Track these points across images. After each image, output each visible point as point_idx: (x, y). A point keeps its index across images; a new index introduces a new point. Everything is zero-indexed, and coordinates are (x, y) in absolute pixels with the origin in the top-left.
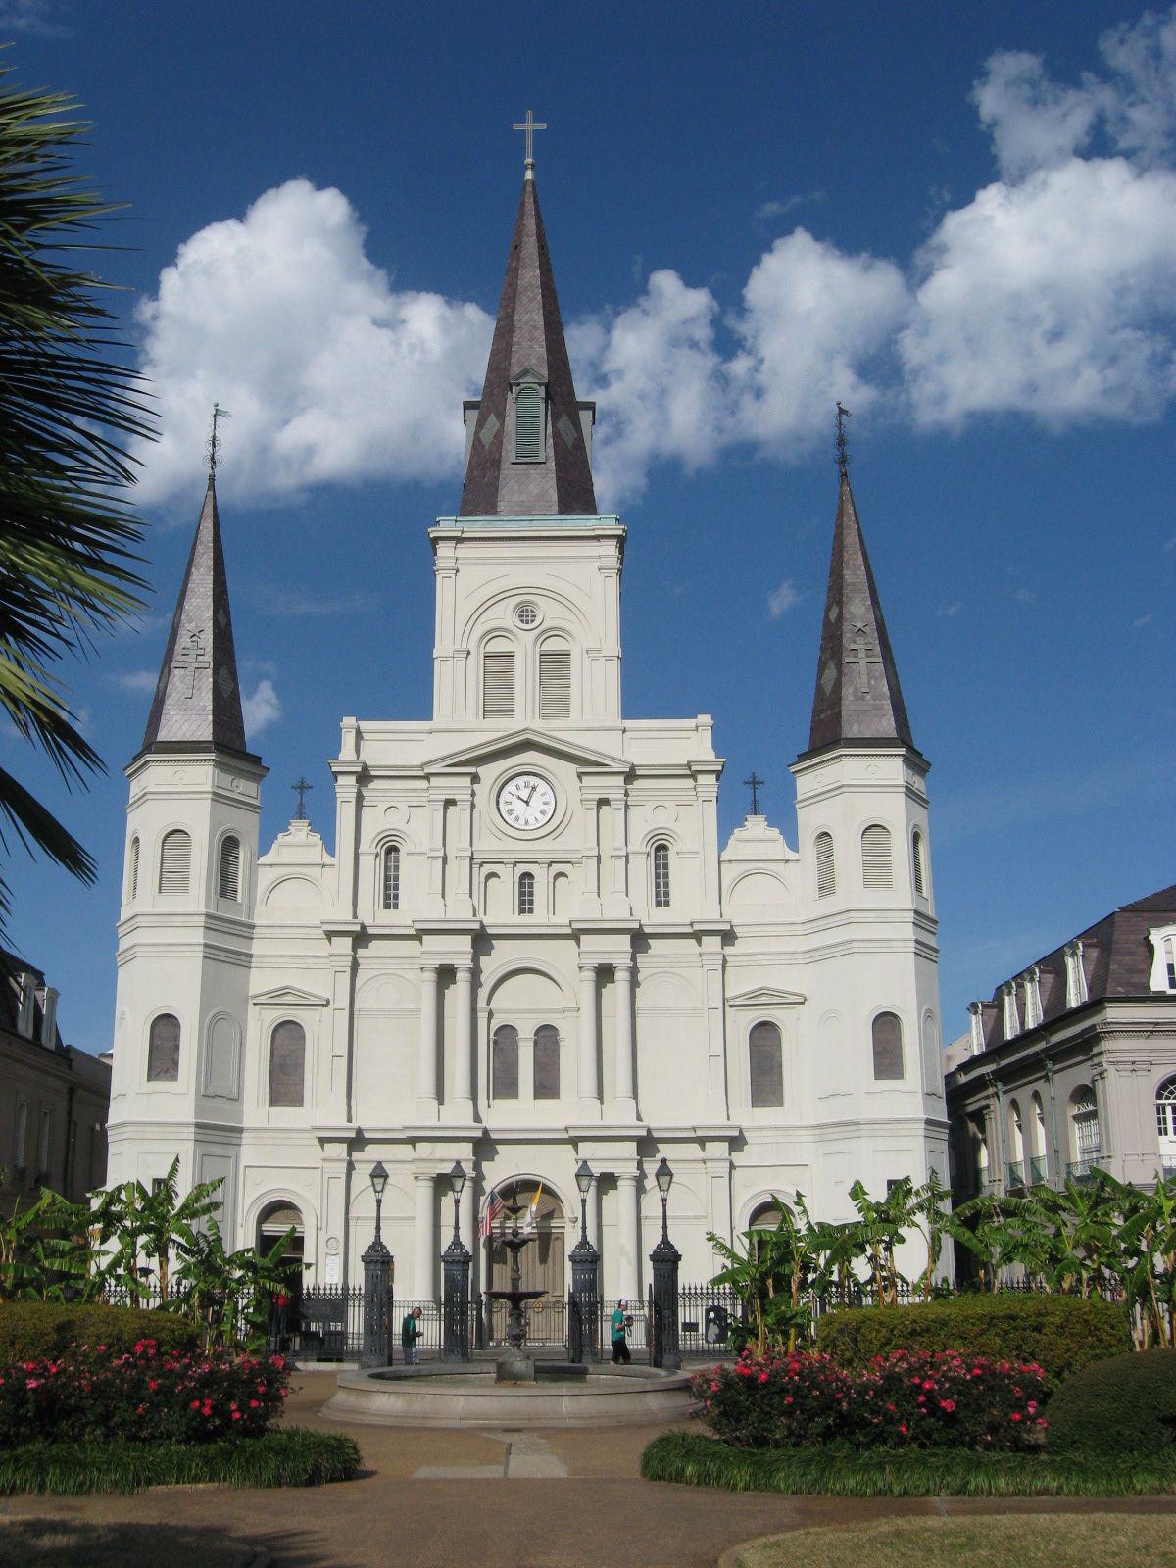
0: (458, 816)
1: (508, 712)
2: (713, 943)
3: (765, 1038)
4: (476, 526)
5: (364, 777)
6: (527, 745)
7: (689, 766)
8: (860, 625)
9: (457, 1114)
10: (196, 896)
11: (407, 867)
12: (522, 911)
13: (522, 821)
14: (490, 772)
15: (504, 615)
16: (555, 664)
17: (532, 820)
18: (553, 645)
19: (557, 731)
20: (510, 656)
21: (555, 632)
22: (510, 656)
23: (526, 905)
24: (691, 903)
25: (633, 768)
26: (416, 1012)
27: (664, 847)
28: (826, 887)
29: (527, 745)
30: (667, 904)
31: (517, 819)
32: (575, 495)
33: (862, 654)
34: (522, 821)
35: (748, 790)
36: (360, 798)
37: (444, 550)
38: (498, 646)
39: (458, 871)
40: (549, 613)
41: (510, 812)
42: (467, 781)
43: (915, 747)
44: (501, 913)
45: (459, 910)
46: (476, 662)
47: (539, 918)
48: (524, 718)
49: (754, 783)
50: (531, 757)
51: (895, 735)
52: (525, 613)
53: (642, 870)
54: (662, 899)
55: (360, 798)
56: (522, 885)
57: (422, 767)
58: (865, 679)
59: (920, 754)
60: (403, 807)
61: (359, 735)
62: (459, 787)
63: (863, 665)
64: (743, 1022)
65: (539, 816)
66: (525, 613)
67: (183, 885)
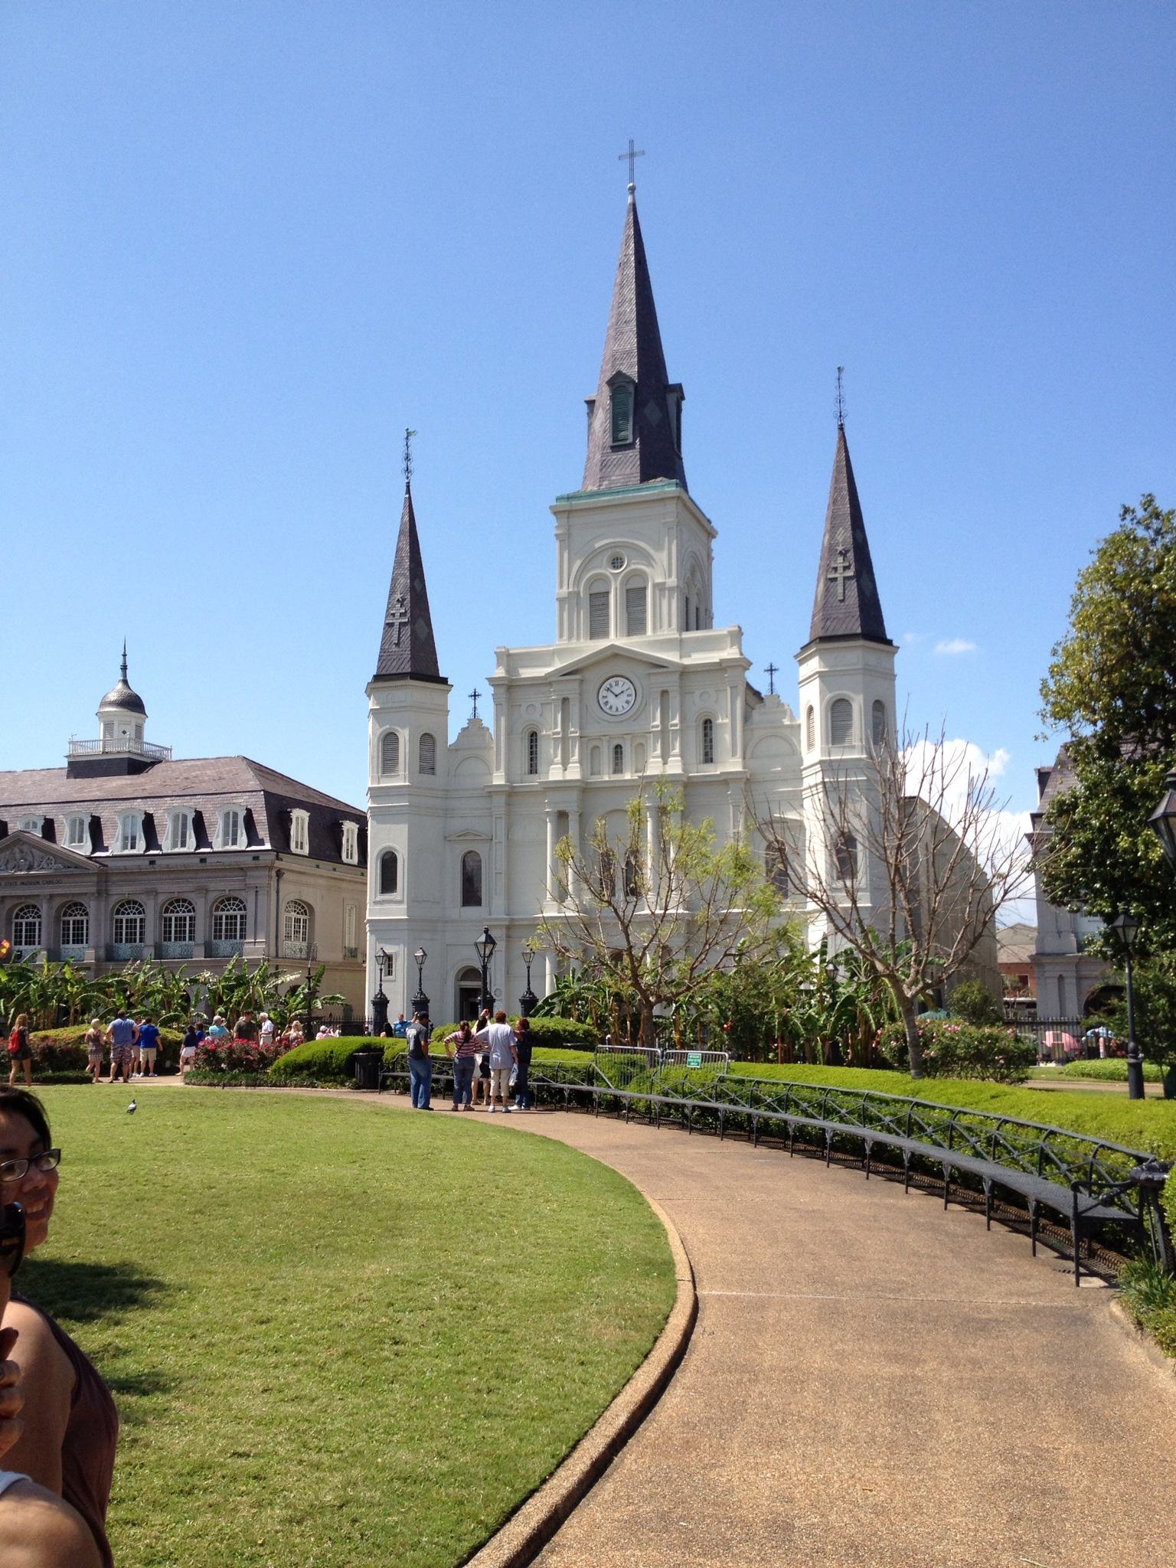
1: (605, 634)
6: (615, 655)
8: (840, 548)
12: (615, 772)
13: (614, 709)
16: (635, 598)
17: (620, 708)
27: (711, 722)
31: (611, 708)
33: (840, 570)
34: (614, 709)
35: (768, 674)
43: (889, 637)
45: (574, 773)
47: (627, 776)
49: (771, 670)
50: (619, 667)
51: (859, 631)
52: (616, 562)
53: (695, 737)
54: (708, 758)
56: (616, 753)
58: (840, 590)
59: (889, 643)
60: (538, 706)
62: (571, 689)
63: (840, 581)
65: (625, 705)
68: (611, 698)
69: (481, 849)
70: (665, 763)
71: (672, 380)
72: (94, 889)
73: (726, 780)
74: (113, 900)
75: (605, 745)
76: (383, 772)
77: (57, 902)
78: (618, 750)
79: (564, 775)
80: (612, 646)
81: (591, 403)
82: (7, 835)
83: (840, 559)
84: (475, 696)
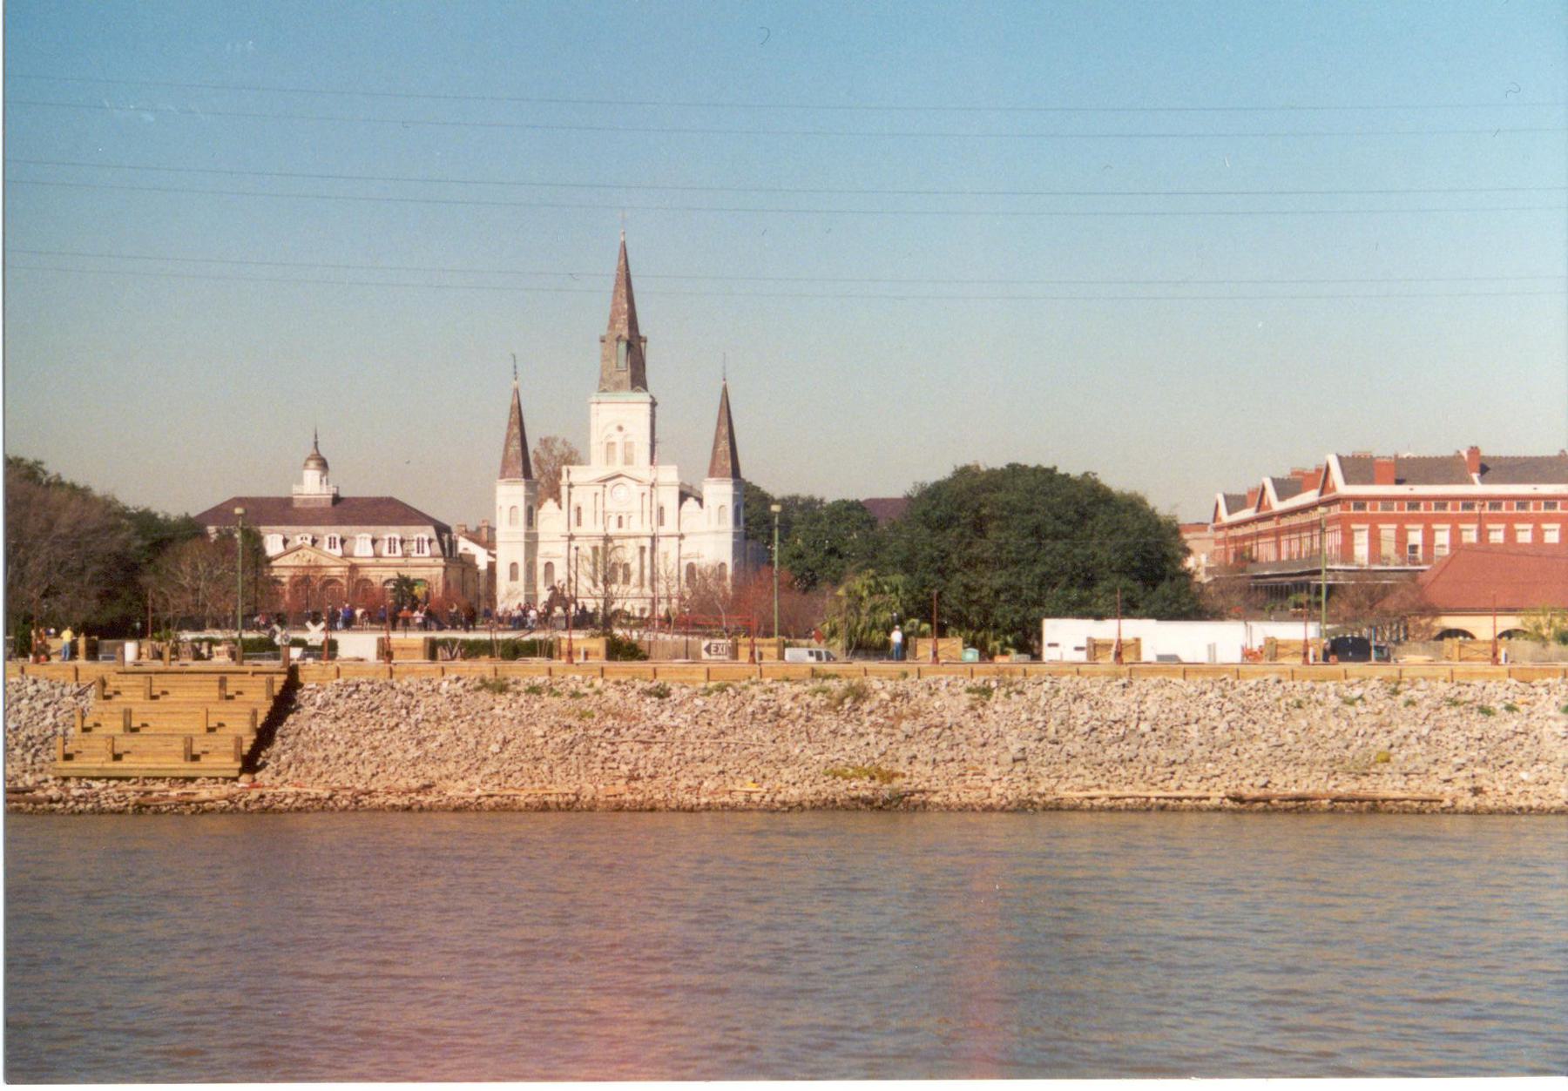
0: (599, 498)
4: (604, 397)
5: (571, 486)
6: (619, 476)
10: (521, 527)
11: (584, 516)
14: (609, 484)
15: (613, 429)
18: (629, 440)
23: (620, 525)
24: (670, 526)
29: (619, 476)
32: (638, 380)
36: (569, 494)
37: (593, 407)
38: (611, 440)
39: (600, 515)
44: (613, 530)
45: (600, 530)
46: (604, 445)
47: (623, 531)
48: (618, 467)
52: (620, 428)
55: (569, 494)
61: (569, 472)
62: (599, 489)
66: (620, 428)
71: (642, 333)
78: (620, 518)
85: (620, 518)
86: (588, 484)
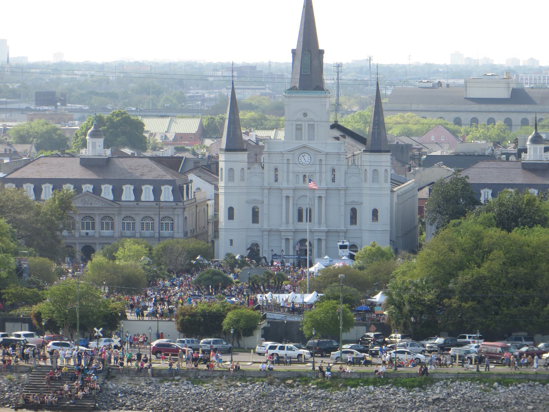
2: (342, 192)
3: (354, 212)
7: (338, 153)
9: (291, 227)
11: (279, 173)
15: (300, 115)
16: (311, 127)
19: (313, 144)
20: (302, 125)
21: (311, 120)
22: (302, 125)
25: (327, 152)
26: (282, 204)
28: (365, 180)
30: (334, 182)
33: (376, 130)
40: (310, 116)
41: (301, 161)
42: (292, 156)
48: (304, 142)
52: (305, 115)
54: (333, 180)
56: (304, 177)
57: (281, 152)
62: (290, 157)
64: (350, 207)
66: (305, 115)
67: (233, 180)
68: (303, 160)
69: (259, 206)
70: (320, 182)
72: (116, 213)
73: (338, 190)
74: (123, 216)
75: (301, 174)
76: (229, 181)
77: (102, 216)
79: (288, 185)
80: (304, 144)
81: (294, 52)
82: (82, 193)
83: (376, 126)
84: (256, 155)
85: (305, 176)
86: (282, 153)
